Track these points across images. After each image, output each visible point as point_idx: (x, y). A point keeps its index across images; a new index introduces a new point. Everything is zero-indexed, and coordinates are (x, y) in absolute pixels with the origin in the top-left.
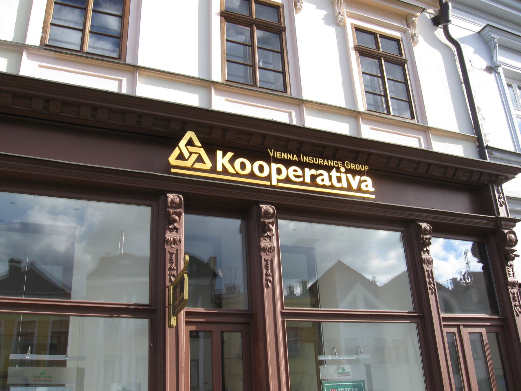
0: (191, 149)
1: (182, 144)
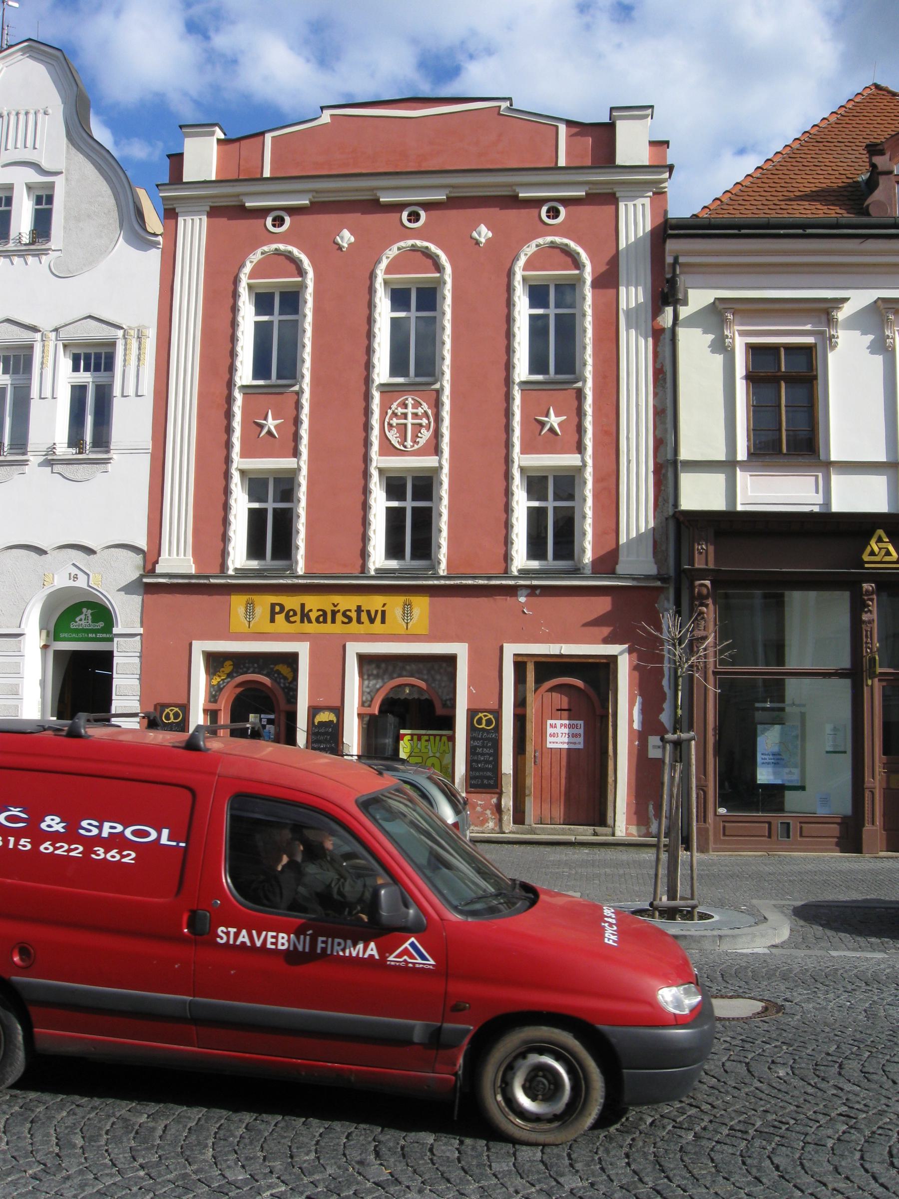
0: (881, 545)
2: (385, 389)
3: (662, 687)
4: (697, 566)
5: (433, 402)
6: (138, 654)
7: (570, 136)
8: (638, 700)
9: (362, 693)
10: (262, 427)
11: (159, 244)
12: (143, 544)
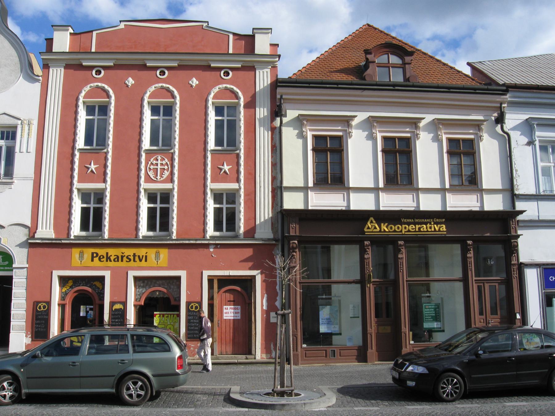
0: (372, 224)
1: (369, 223)
2: (148, 152)
3: (276, 289)
4: (291, 234)
5: (170, 159)
6: (25, 277)
7: (234, 40)
8: (266, 296)
9: (136, 295)
10: (88, 168)
11: (40, 80)
12: (29, 224)
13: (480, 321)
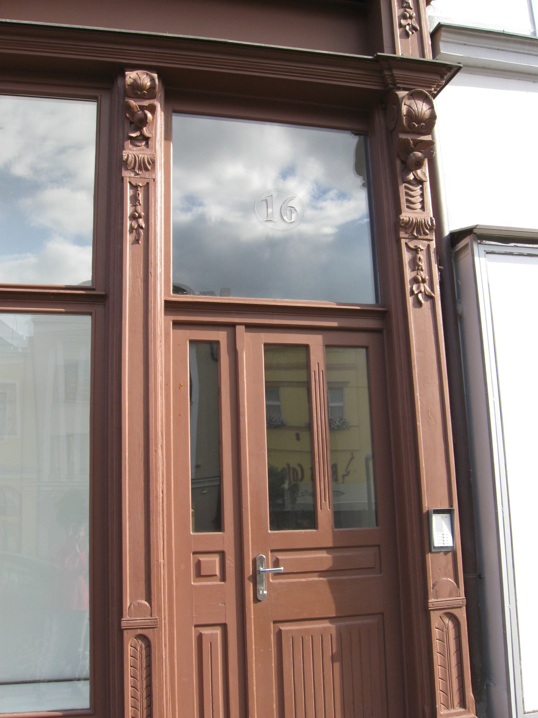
13: (198, 565)
